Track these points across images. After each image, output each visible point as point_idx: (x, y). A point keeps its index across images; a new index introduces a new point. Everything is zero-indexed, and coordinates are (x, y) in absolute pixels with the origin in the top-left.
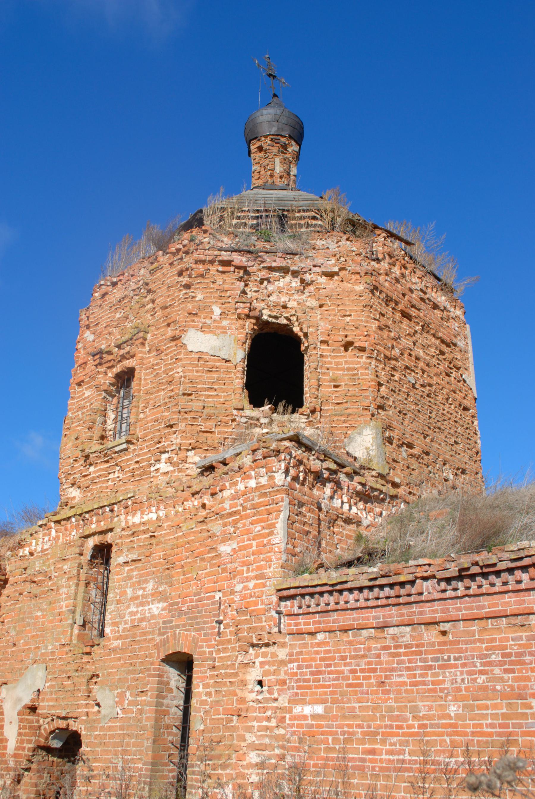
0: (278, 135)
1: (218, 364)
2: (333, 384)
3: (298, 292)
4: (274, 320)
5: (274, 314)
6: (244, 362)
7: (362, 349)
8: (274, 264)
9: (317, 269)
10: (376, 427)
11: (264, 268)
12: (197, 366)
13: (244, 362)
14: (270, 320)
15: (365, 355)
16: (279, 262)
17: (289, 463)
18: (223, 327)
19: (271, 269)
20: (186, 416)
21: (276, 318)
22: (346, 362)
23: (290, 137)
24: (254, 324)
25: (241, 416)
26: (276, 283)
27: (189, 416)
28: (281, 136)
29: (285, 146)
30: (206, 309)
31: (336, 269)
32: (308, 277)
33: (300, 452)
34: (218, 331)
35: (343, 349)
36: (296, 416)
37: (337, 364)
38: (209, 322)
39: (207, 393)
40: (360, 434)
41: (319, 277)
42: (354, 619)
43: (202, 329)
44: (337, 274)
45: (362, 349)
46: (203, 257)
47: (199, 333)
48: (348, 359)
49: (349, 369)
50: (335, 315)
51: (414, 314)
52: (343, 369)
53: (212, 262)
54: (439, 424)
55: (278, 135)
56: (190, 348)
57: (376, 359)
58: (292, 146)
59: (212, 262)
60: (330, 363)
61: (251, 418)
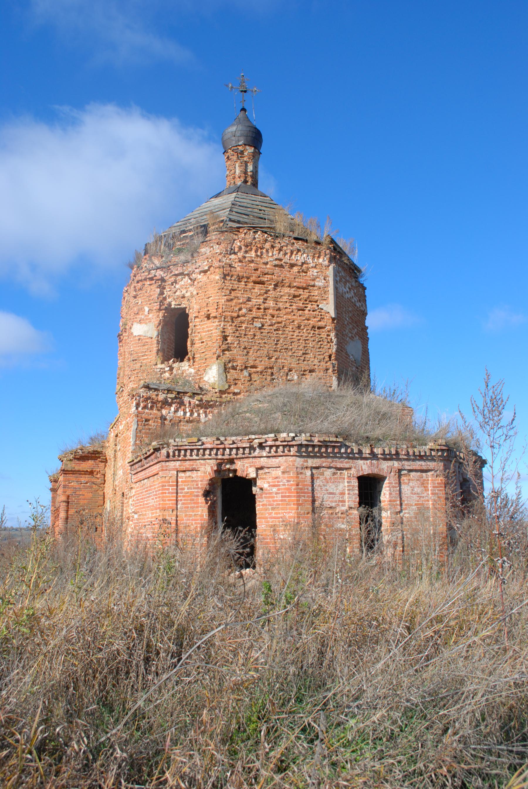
0: (236, 146)
1: (147, 340)
2: (200, 341)
3: (191, 285)
4: (178, 307)
5: (177, 303)
6: (158, 337)
7: (215, 317)
8: (177, 272)
9: (197, 271)
10: (219, 364)
11: (173, 275)
12: (138, 343)
13: (158, 337)
14: (176, 307)
15: (217, 320)
16: (180, 270)
17: (139, 401)
18: (149, 319)
19: (176, 275)
20: (134, 372)
21: (179, 305)
22: (207, 327)
23: (245, 145)
24: (165, 313)
25: (157, 369)
26: (180, 283)
27: (135, 372)
28: (239, 145)
29: (242, 153)
30: (141, 309)
31: (206, 268)
32: (194, 276)
33: (151, 392)
34: (147, 321)
35: (206, 319)
36: (183, 364)
37: (203, 329)
38: (143, 317)
39: (143, 358)
40: (210, 369)
41: (198, 275)
42: (141, 476)
43: (140, 322)
44: (209, 270)
45: (215, 317)
46: (140, 278)
47: (139, 325)
48: (208, 325)
49: (208, 331)
50: (202, 299)
51: (266, 279)
52: (206, 332)
53: (145, 279)
54: (285, 347)
55: (236, 146)
56: (134, 334)
57: (224, 321)
58: (247, 150)
59: (145, 279)
60: (200, 329)
61: (161, 369)
